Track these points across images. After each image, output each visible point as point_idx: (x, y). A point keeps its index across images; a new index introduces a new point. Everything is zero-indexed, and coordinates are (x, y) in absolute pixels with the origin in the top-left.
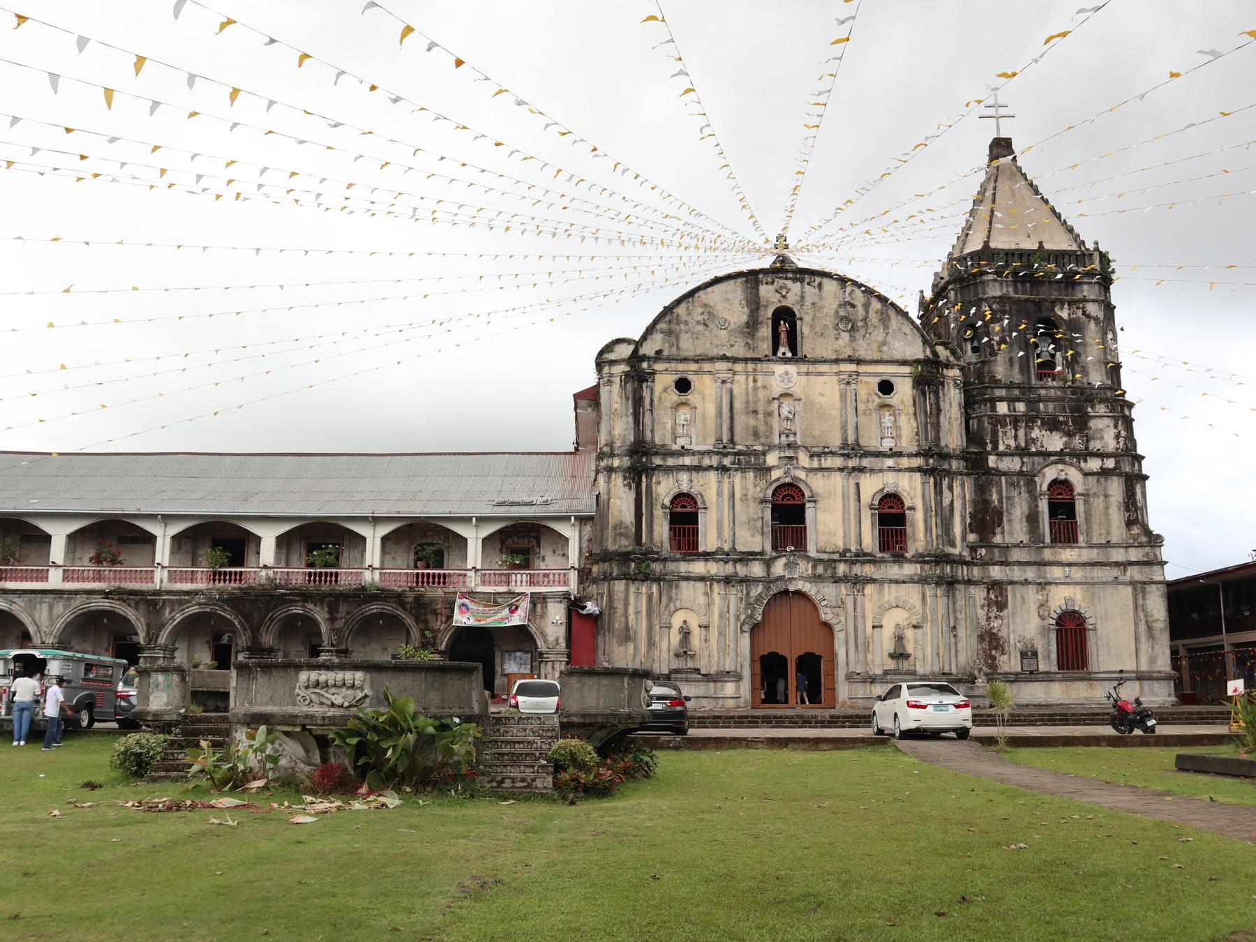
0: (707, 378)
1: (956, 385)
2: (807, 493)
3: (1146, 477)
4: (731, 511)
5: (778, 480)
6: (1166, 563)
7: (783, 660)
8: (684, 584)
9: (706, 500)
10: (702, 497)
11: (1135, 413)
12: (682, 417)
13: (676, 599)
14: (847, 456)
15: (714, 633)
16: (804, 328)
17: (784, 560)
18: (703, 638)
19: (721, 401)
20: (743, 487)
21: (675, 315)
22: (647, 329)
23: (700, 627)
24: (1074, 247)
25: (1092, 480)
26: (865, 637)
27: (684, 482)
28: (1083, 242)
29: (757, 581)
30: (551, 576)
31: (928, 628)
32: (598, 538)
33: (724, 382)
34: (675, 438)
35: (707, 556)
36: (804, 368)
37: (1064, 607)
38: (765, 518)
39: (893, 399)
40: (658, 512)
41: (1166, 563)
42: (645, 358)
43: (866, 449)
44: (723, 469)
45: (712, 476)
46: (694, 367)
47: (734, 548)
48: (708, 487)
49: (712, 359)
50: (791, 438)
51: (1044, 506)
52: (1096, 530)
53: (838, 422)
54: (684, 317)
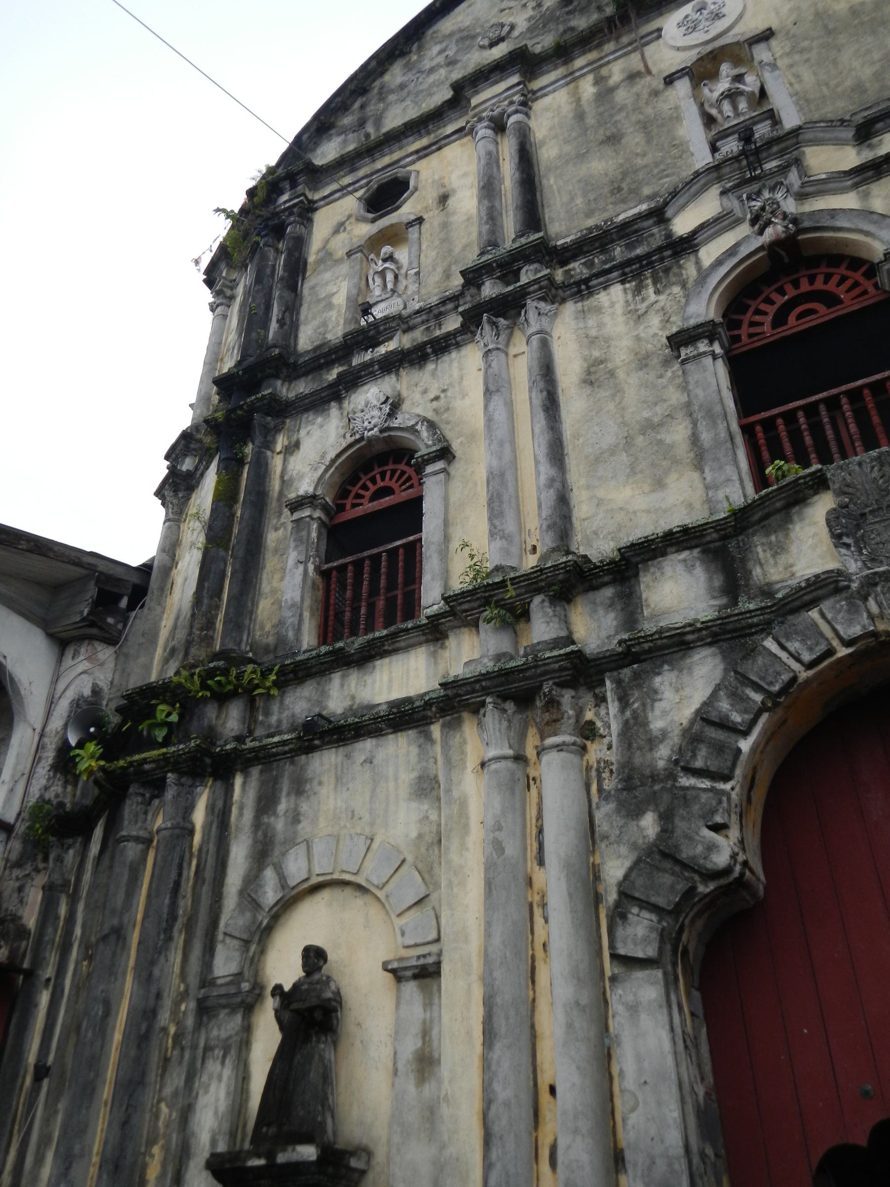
9: (449, 435)
13: (291, 842)
18: (410, 1046)
22: (298, 138)
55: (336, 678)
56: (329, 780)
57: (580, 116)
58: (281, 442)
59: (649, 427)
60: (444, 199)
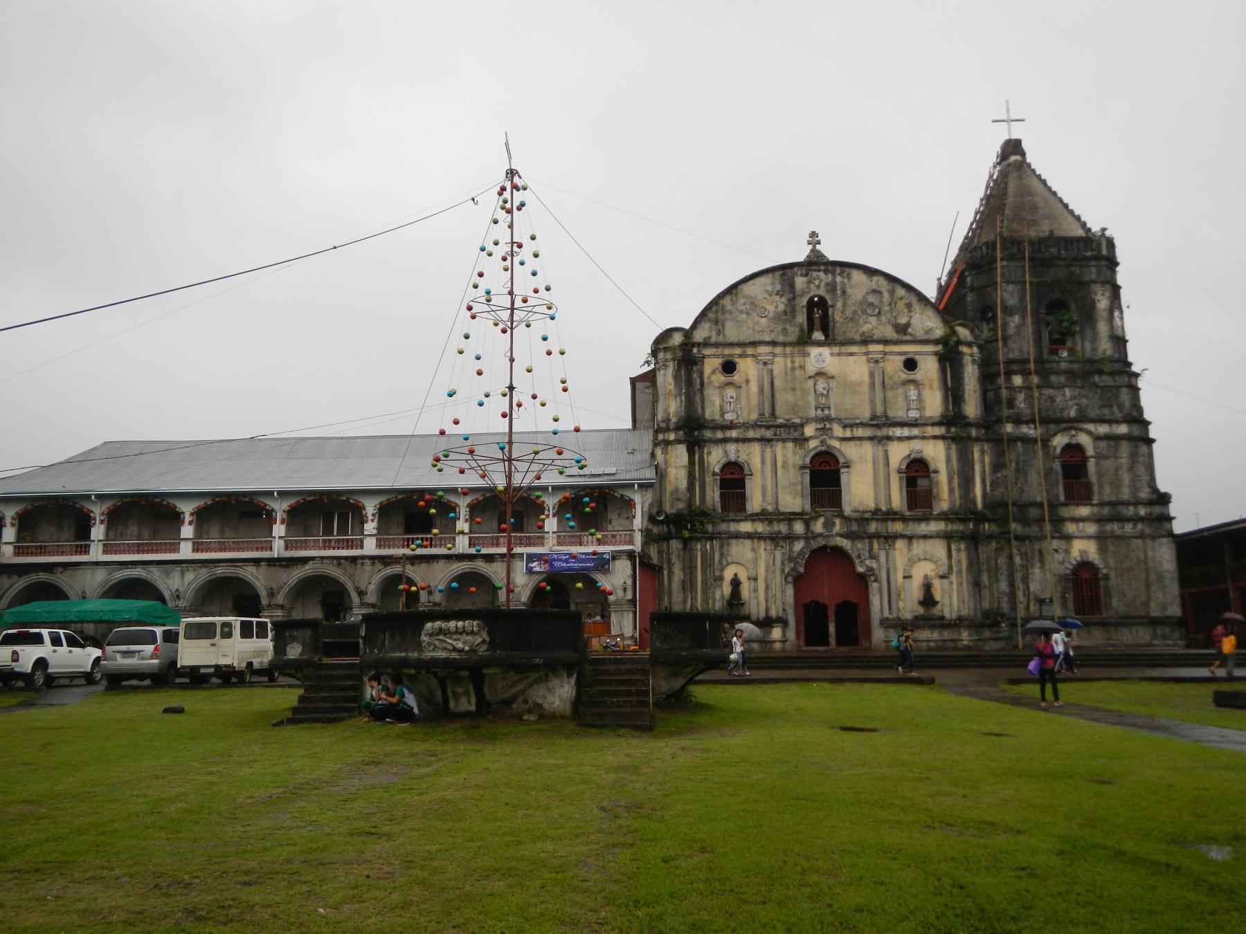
0: (749, 361)
1: (974, 362)
2: (842, 460)
3: (1153, 441)
4: (774, 478)
5: (815, 448)
6: (1173, 518)
7: (824, 608)
8: (734, 542)
10: (748, 465)
11: (1141, 383)
12: (729, 395)
13: (728, 555)
14: (877, 426)
15: (761, 585)
16: (837, 315)
17: (822, 520)
18: (752, 589)
19: (763, 381)
20: (785, 456)
21: (721, 306)
22: (696, 319)
23: (749, 579)
24: (1080, 233)
25: (1102, 444)
26: (896, 587)
27: (733, 451)
28: (1089, 230)
29: (798, 538)
30: (618, 536)
31: (954, 578)
32: (659, 503)
33: (765, 364)
34: (723, 413)
35: (754, 518)
36: (836, 350)
37: (1079, 559)
38: (805, 482)
39: (918, 375)
40: (709, 479)
41: (1173, 518)
42: (693, 345)
43: (894, 420)
44: (763, 440)
45: (756, 448)
46: (738, 351)
47: (777, 509)
48: (752, 456)
49: (754, 344)
50: (826, 412)
51: (1057, 466)
52: (1107, 490)
53: (867, 397)
54: (728, 307)
55: (732, 524)
56: (734, 546)
57: (786, 373)
58: (706, 452)
59: (794, 484)
60: (747, 381)
